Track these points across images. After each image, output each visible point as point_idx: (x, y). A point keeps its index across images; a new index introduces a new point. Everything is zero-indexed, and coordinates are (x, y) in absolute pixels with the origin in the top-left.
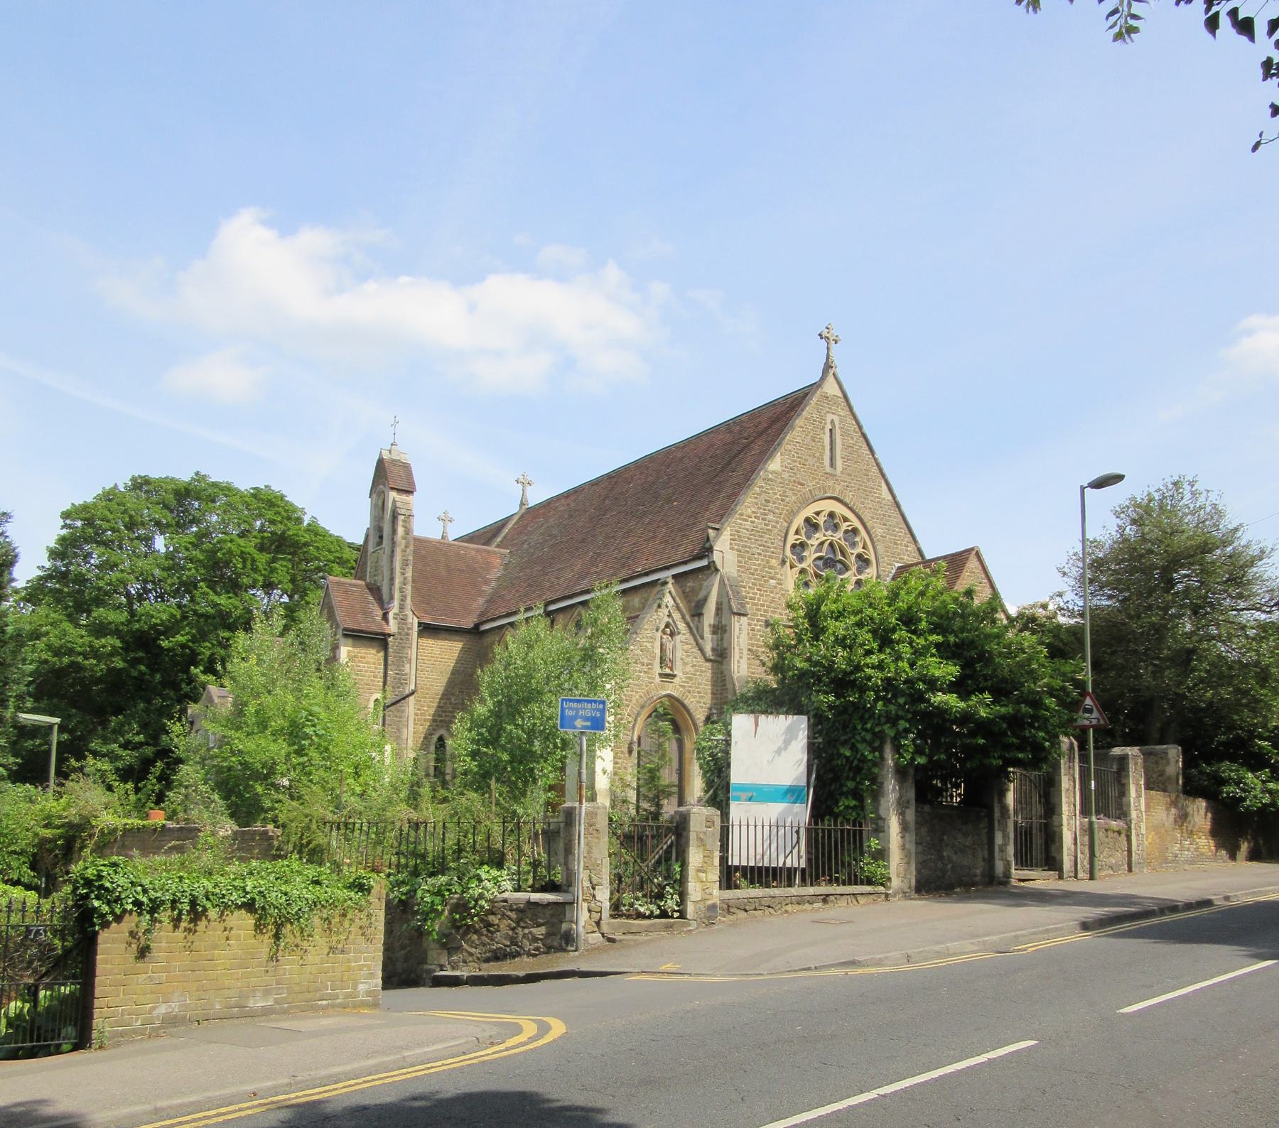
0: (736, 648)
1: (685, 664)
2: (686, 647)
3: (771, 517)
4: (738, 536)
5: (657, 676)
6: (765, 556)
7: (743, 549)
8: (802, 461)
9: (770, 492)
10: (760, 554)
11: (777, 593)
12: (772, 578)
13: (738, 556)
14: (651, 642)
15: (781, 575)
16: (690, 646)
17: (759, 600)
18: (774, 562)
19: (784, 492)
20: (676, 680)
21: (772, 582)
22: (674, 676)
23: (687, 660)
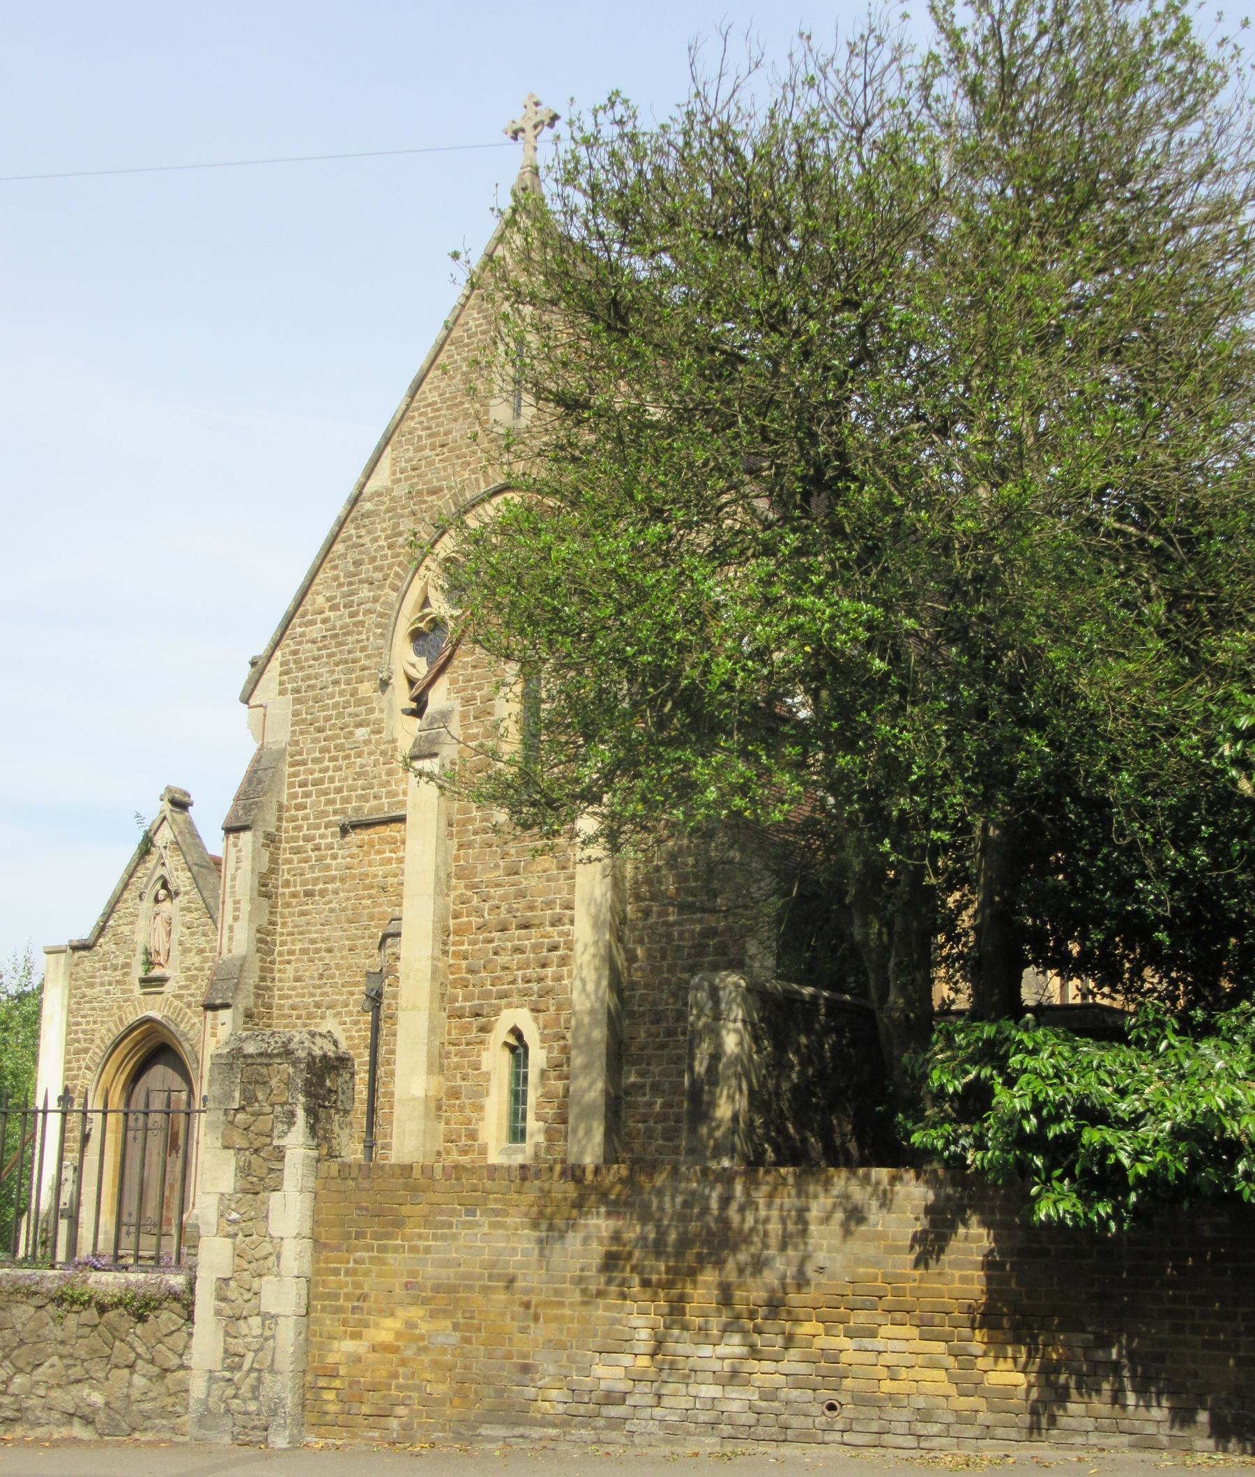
0: (229, 902)
1: (186, 951)
2: (188, 918)
3: (365, 592)
4: (296, 662)
5: (137, 983)
6: (348, 683)
7: (303, 685)
8: (438, 440)
9: (366, 540)
10: (336, 682)
11: (370, 754)
12: (359, 725)
13: (297, 701)
14: (132, 923)
15: (382, 711)
16: (196, 915)
17: (332, 780)
18: (366, 689)
19: (396, 525)
20: (168, 988)
21: (361, 733)
22: (162, 981)
23: (189, 942)
